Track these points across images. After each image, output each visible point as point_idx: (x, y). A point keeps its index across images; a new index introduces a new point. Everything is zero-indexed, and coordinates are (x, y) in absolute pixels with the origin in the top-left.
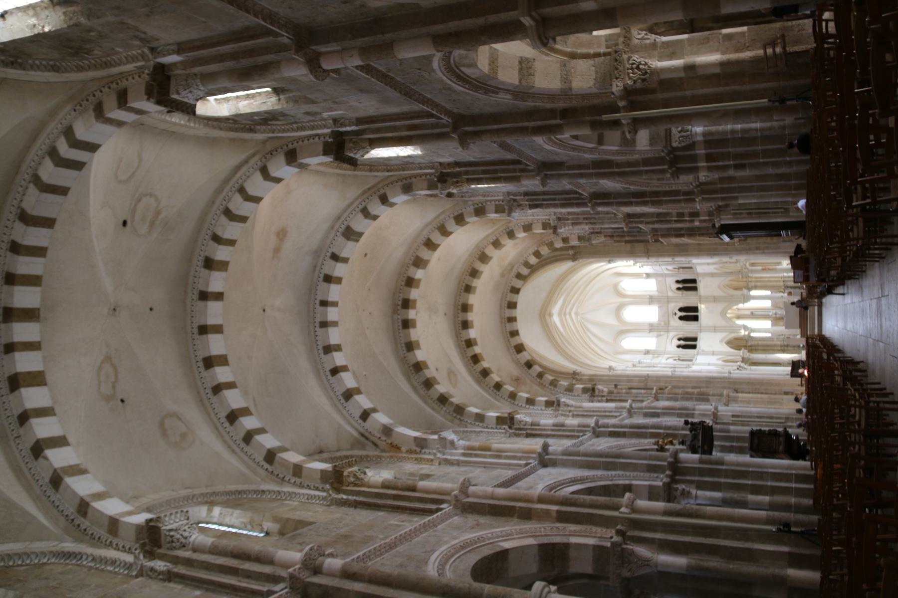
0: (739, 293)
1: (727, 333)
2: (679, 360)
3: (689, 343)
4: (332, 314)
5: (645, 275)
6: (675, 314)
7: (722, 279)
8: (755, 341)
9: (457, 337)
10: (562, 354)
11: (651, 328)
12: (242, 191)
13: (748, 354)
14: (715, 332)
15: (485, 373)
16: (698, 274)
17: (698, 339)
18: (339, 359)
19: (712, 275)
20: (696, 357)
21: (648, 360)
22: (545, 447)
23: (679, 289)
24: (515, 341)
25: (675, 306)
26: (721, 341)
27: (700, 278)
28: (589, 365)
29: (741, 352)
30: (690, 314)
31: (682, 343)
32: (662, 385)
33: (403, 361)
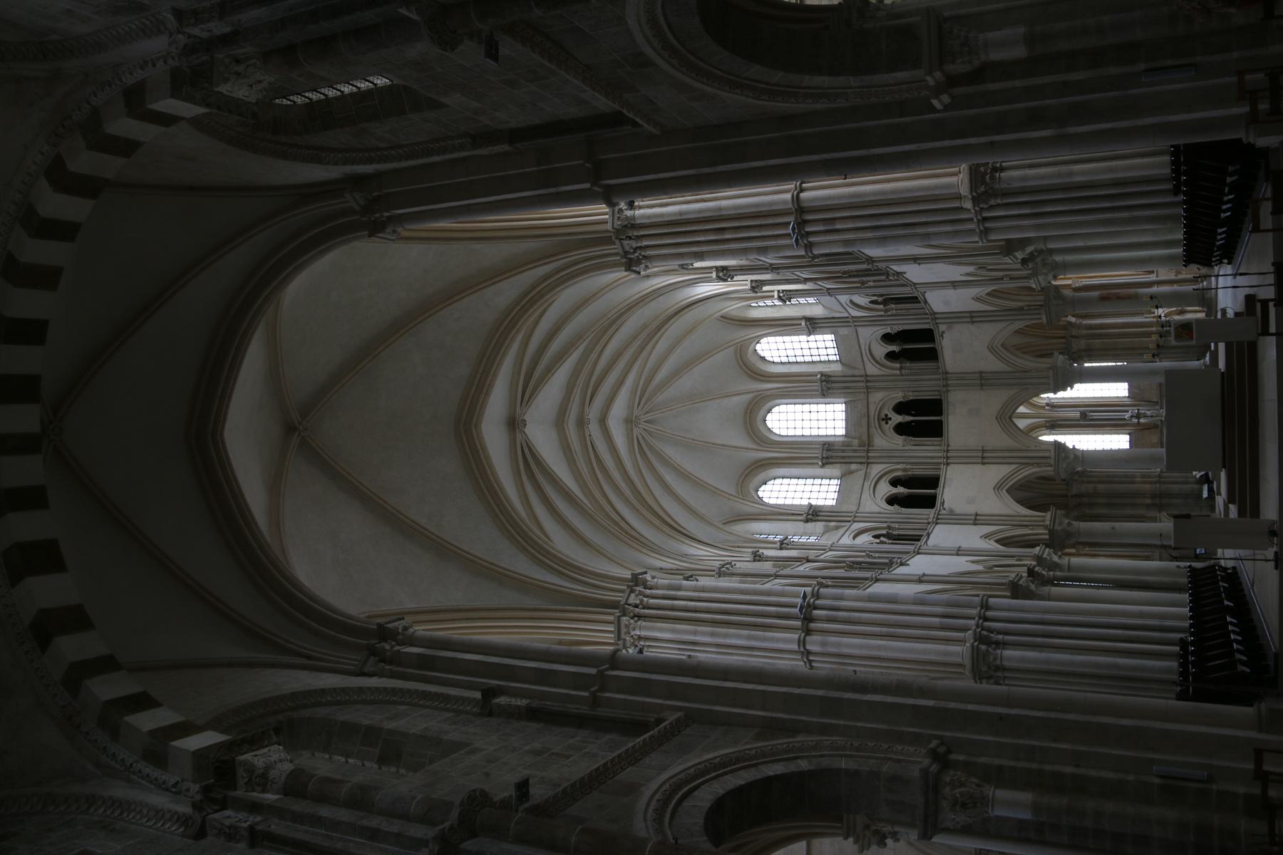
0: (1044, 363)
1: (1014, 466)
2: (888, 536)
5: (803, 323)
6: (887, 419)
7: (1001, 325)
8: (1090, 482)
13: (1067, 521)
14: (983, 464)
16: (934, 315)
17: (942, 480)
19: (972, 317)
20: (930, 528)
25: (884, 399)
26: (998, 487)
27: (942, 328)
28: (580, 570)
29: (1048, 515)
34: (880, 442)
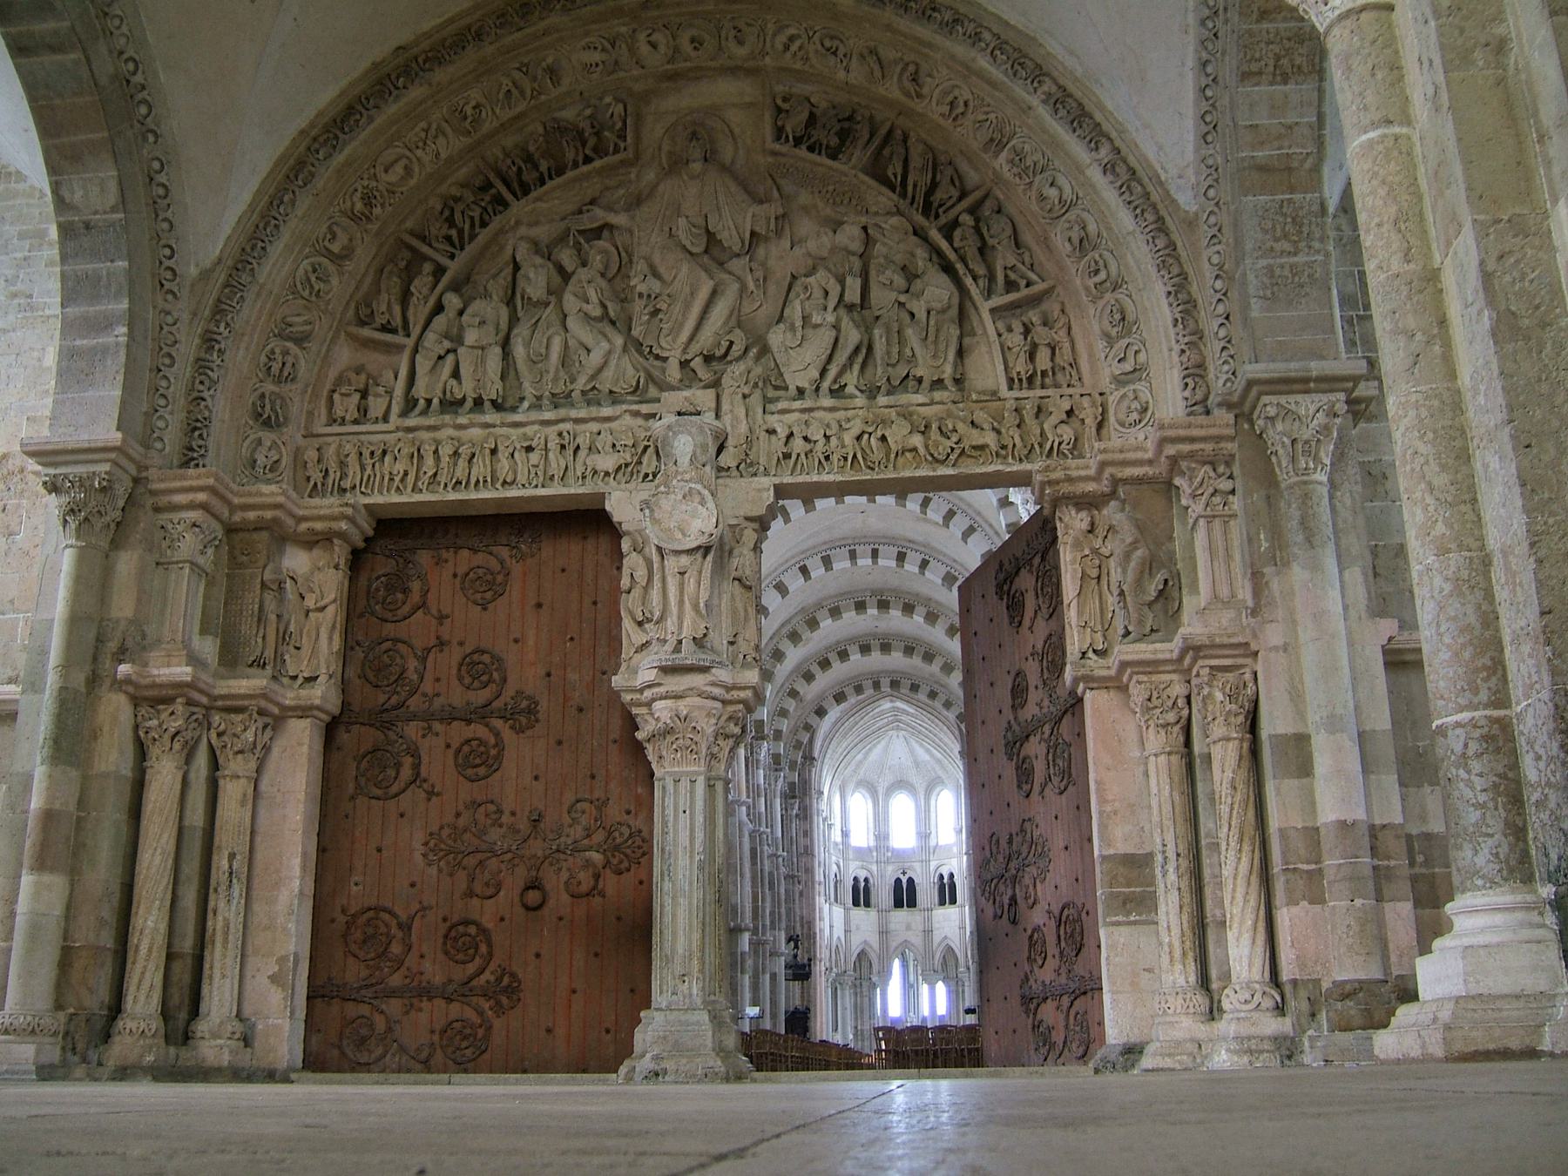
3: (861, 895)
4: (865, 562)
6: (904, 873)
9: (852, 640)
10: (836, 723)
11: (882, 836)
12: (970, 531)
15: (809, 677)
18: (817, 571)
21: (836, 836)
22: (744, 803)
23: (941, 877)
24: (849, 691)
30: (905, 895)
31: (863, 884)
32: (803, 877)
33: (819, 606)
34: (890, 868)
